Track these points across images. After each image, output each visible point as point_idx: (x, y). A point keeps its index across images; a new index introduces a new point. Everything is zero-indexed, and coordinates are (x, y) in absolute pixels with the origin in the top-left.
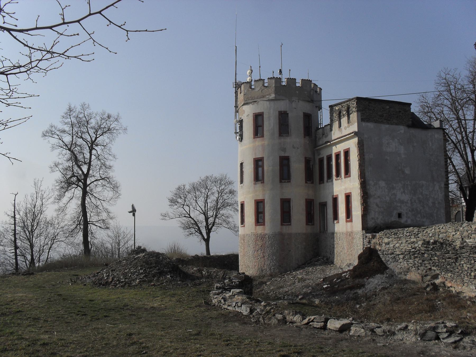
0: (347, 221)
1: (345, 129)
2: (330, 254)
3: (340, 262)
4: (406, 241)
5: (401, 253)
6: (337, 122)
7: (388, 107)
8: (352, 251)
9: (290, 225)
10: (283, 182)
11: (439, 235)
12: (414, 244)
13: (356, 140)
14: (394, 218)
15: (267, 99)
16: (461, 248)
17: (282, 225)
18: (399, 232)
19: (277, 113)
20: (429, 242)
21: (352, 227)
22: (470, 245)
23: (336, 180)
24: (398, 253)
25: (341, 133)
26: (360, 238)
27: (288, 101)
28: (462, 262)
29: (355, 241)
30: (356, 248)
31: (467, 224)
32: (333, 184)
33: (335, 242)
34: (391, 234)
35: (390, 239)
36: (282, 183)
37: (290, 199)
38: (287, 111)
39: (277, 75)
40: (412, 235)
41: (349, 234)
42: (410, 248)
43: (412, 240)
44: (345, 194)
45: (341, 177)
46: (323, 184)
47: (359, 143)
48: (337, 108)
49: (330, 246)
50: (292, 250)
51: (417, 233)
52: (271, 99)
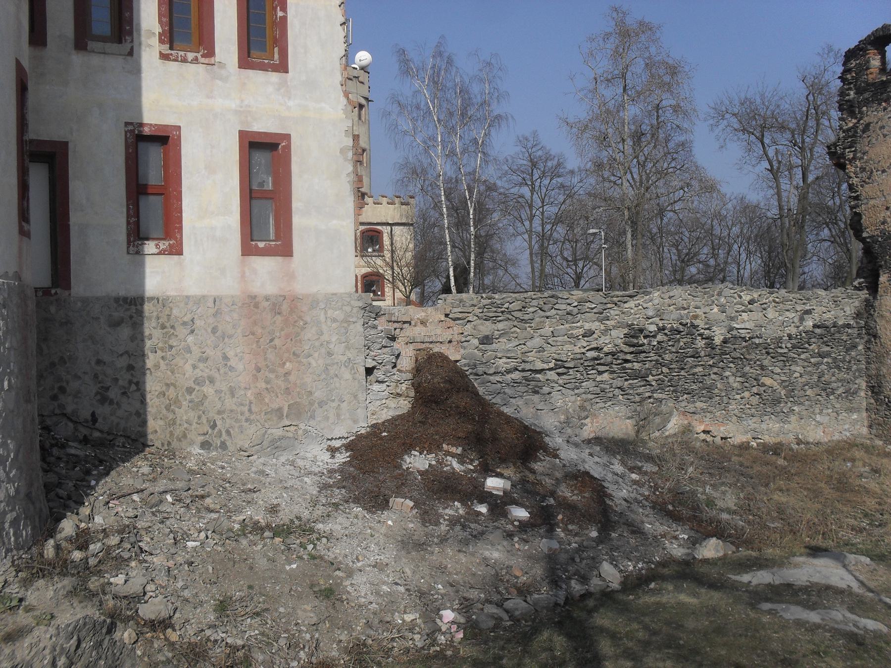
0: (248, 250)
2: (104, 399)
3: (206, 428)
5: (552, 365)
8: (287, 374)
16: (725, 341)
21: (291, 276)
22: (743, 336)
23: (164, 57)
24: (539, 365)
26: (346, 321)
28: (727, 373)
29: (310, 333)
30: (321, 362)
31: (732, 291)
32: (137, 71)
33: (148, 344)
41: (266, 304)
42: (583, 350)
43: (587, 326)
44: (243, 134)
45: (210, 52)
49: (99, 362)
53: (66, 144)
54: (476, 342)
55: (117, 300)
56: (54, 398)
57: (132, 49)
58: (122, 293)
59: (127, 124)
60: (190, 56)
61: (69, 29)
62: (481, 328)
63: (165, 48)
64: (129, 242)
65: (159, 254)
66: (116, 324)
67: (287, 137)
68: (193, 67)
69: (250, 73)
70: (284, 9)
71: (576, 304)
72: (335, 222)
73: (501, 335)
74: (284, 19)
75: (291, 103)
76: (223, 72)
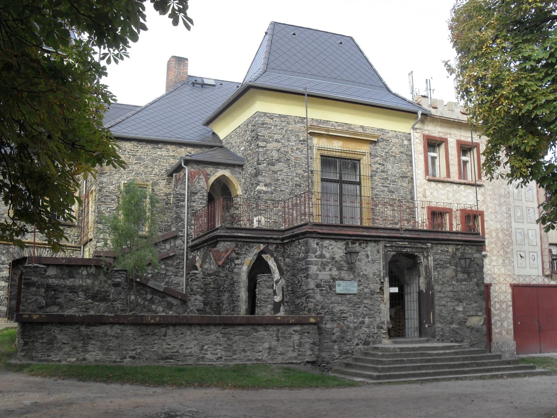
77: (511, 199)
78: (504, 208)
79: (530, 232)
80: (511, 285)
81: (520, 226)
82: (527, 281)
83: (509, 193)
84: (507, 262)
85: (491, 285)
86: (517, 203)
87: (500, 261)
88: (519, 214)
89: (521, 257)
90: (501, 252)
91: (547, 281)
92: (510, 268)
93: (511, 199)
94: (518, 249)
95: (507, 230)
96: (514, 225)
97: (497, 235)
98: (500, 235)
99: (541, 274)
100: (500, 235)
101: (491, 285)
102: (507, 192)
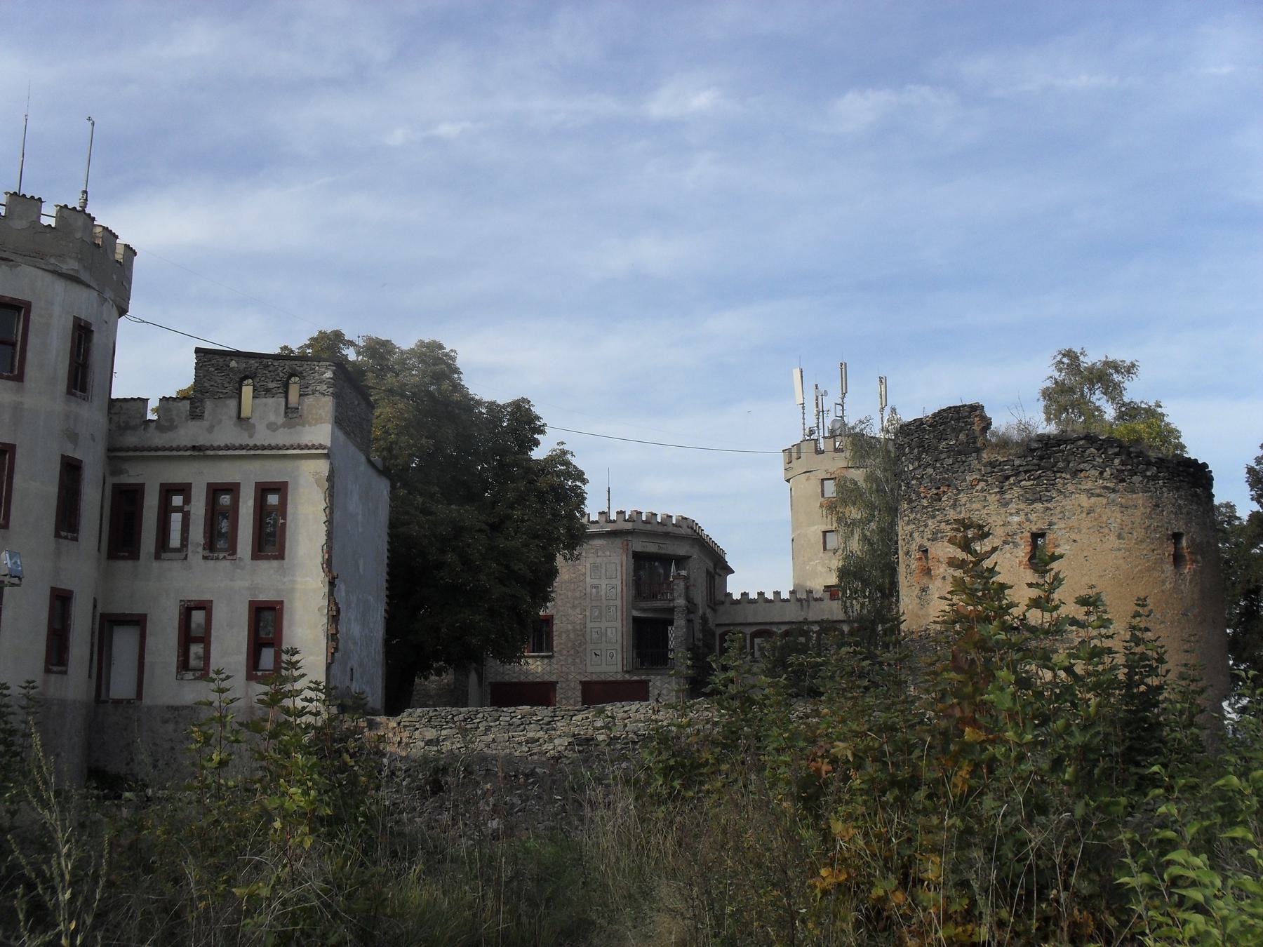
0: (250, 677)
1: (272, 427)
4: (509, 738)
6: (233, 403)
7: (356, 403)
9: (65, 673)
10: (60, 537)
11: (625, 726)
12: (540, 745)
13: (323, 467)
14: (347, 683)
15: (51, 268)
17: (48, 671)
18: (480, 715)
19: (70, 325)
20: (589, 740)
23: (205, 558)
25: (251, 436)
27: (95, 294)
34: (452, 718)
35: (444, 732)
36: (60, 540)
37: (71, 592)
38: (91, 324)
39: (75, 203)
40: (530, 723)
43: (531, 735)
44: (251, 603)
45: (232, 549)
46: (130, 563)
47: (330, 478)
48: (233, 364)
49: (155, 744)
50: (63, 754)
51: (547, 719)
52: (64, 271)
53: (145, 615)
54: (422, 744)
55: (168, 707)
56: (128, 764)
57: (187, 555)
58: (172, 703)
59: (181, 601)
60: (221, 556)
61: (152, 549)
62: (426, 734)
63: (207, 553)
64: (177, 672)
65: (195, 679)
66: (166, 721)
67: (282, 602)
68: (225, 561)
69: (259, 562)
70: (284, 517)
71: (520, 717)
72: (312, 658)
73: (443, 740)
74: (284, 525)
75: (285, 580)
76: (242, 564)
77: (588, 600)
78: (578, 610)
79: (609, 630)
80: (580, 682)
81: (596, 625)
82: (603, 678)
83: (585, 594)
84: (578, 661)
85: (557, 682)
86: (594, 604)
87: (570, 660)
88: (596, 614)
89: (596, 654)
90: (572, 652)
91: (627, 677)
92: (581, 666)
93: (588, 600)
94: (592, 647)
95: (581, 630)
96: (589, 625)
97: (568, 636)
98: (572, 636)
99: (620, 669)
100: (572, 636)
101: (557, 682)
102: (582, 594)
